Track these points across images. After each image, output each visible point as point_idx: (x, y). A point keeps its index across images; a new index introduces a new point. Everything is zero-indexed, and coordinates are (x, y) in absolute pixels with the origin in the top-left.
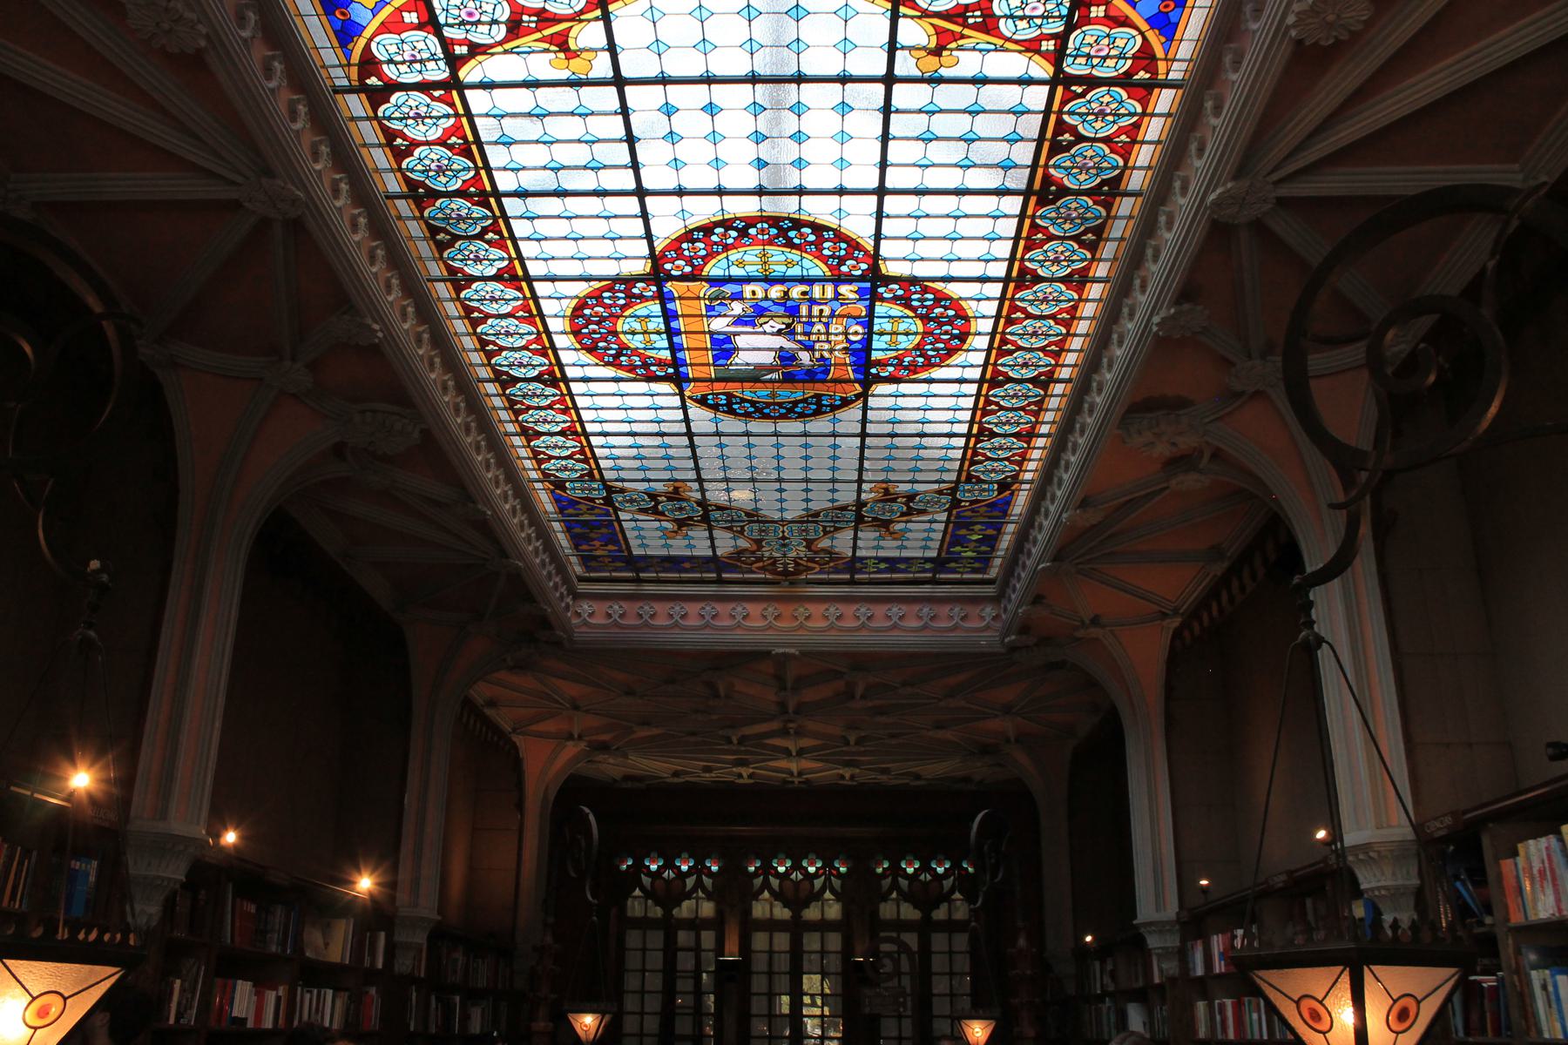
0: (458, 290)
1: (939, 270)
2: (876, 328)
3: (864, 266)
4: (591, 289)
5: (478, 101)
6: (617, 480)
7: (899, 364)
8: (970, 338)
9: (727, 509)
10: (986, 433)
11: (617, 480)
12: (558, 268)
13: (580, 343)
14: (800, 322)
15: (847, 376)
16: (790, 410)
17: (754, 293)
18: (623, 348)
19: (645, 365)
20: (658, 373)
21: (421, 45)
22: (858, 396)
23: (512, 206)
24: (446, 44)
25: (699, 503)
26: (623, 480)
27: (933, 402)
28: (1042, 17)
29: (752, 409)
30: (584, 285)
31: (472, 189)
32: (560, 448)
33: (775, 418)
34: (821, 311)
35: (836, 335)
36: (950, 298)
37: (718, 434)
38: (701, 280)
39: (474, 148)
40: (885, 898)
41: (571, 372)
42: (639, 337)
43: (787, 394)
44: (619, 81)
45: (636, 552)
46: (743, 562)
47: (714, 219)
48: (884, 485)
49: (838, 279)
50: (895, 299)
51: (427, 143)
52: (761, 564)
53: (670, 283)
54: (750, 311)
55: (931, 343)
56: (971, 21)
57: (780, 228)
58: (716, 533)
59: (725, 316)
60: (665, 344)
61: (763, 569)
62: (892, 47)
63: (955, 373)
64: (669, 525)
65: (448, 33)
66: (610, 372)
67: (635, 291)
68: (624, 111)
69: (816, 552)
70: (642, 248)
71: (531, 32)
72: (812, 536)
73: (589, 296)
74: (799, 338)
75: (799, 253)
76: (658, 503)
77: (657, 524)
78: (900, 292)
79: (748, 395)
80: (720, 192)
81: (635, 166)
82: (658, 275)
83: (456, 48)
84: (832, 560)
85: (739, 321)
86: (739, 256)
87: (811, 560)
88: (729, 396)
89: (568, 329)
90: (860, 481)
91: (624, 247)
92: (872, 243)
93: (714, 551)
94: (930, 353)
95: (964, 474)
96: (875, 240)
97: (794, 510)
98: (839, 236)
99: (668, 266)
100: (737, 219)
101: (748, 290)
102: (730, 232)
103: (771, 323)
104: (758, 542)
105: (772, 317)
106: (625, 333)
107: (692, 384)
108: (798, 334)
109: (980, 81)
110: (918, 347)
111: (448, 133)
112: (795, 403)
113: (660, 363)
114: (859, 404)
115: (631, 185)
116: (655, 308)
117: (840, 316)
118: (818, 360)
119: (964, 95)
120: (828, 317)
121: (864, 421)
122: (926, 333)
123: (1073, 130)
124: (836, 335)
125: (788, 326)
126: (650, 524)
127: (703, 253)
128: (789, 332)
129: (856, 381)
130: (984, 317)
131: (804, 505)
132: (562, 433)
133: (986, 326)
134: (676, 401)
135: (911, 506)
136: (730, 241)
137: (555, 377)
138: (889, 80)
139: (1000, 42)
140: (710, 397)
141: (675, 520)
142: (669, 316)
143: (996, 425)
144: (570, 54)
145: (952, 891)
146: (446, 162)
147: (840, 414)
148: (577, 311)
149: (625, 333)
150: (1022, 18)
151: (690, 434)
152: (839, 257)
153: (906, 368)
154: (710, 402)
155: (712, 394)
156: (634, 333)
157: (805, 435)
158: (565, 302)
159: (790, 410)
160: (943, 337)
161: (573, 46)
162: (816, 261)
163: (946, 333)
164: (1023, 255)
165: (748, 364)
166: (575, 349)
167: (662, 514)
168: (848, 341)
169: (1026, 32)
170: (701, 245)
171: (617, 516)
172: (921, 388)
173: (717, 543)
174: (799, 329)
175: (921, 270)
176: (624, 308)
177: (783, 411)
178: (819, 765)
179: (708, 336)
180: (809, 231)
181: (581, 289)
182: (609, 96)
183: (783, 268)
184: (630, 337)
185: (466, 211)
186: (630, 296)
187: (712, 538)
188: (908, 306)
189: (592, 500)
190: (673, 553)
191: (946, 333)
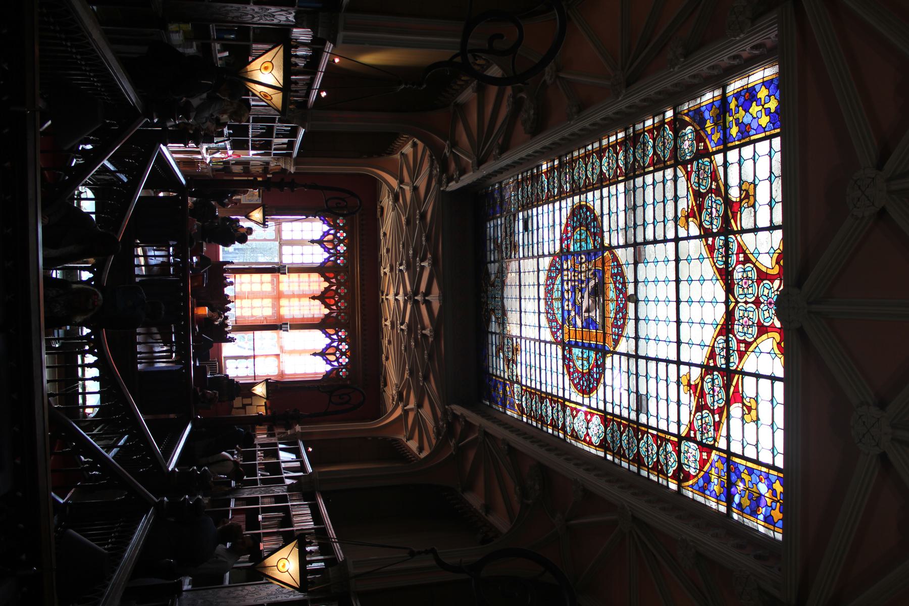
0: (596, 152)
1: (608, 381)
2: (584, 351)
5: (669, 173)
7: (570, 360)
10: (542, 400)
18: (574, 229)
19: (567, 238)
20: (564, 244)
27: (554, 375)
28: (702, 431)
29: (549, 288)
36: (597, 386)
37: (539, 271)
41: (564, 203)
42: (578, 237)
44: (677, 240)
48: (519, 349)
50: (596, 360)
52: (484, 285)
57: (623, 308)
62: (690, 365)
63: (567, 387)
65: (695, 163)
66: (564, 221)
68: (665, 241)
71: (696, 201)
78: (599, 363)
80: (636, 282)
100: (626, 288)
106: (580, 230)
109: (679, 403)
113: (568, 246)
114: (553, 340)
119: (673, 397)
121: (546, 342)
122: (583, 374)
130: (590, 401)
136: (618, 285)
138: (678, 363)
139: (693, 413)
143: (546, 405)
144: (687, 217)
148: (588, 208)
151: (539, 256)
153: (569, 363)
156: (580, 235)
158: (592, 203)
160: (581, 382)
161: (690, 219)
163: (583, 383)
164: (615, 421)
166: (573, 206)
169: (697, 424)
172: (560, 370)
173: (492, 264)
175: (608, 373)
177: (549, 303)
181: (597, 211)
182: (671, 235)
184: (579, 233)
186: (595, 234)
191: (583, 383)
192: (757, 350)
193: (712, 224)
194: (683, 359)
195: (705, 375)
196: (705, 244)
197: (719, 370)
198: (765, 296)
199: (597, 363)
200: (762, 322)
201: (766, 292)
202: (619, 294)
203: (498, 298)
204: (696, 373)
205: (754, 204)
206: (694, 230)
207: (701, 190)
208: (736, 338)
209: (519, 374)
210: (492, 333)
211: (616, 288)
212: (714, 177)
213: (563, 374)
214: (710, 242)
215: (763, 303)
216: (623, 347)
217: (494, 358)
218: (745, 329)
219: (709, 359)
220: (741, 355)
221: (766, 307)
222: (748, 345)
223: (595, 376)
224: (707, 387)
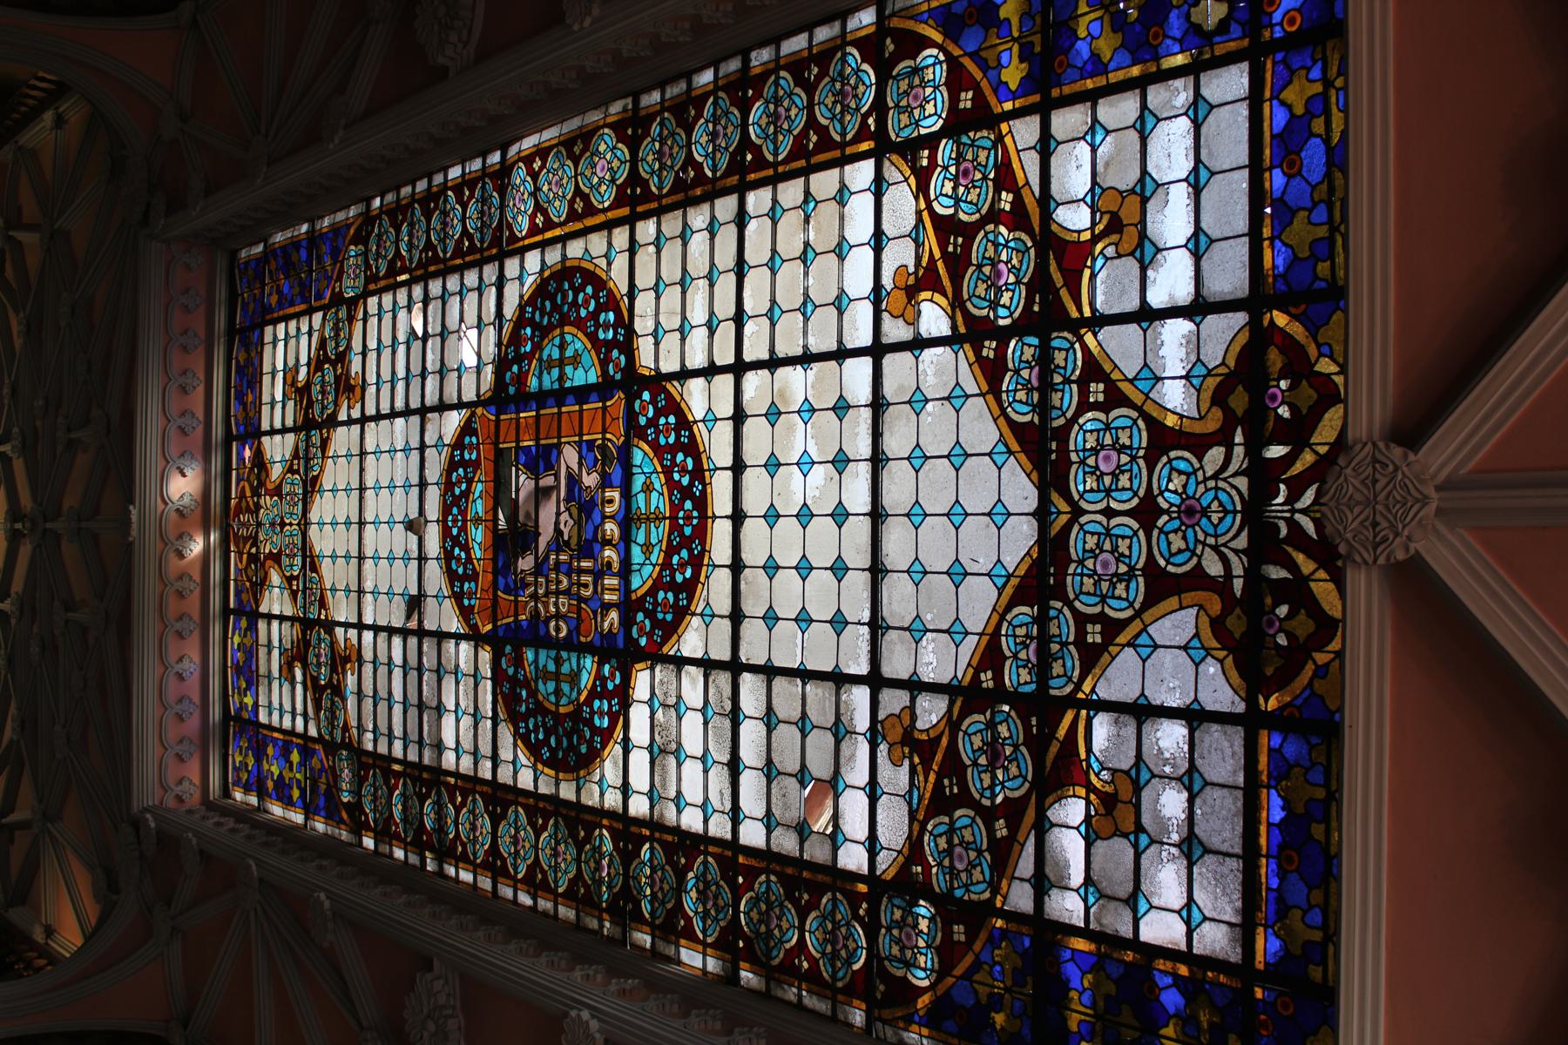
2: (564, 654)
3: (643, 642)
4: (619, 297)
6: (366, 312)
8: (552, 773)
9: (323, 452)
11: (366, 312)
12: (645, 257)
13: (552, 276)
14: (571, 557)
15: (500, 617)
17: (611, 501)
19: (519, 358)
20: (509, 374)
21: (930, 109)
22: (474, 628)
23: (726, 207)
24: (932, 141)
25: (334, 415)
26: (365, 321)
29: (457, 491)
30: (624, 289)
31: (749, 157)
32: (410, 241)
33: (445, 521)
34: (586, 586)
35: (556, 604)
38: (627, 435)
39: (802, 163)
41: (512, 266)
42: (556, 354)
44: (878, 350)
45: (269, 330)
46: (251, 469)
47: (704, 457)
48: (354, 658)
49: (629, 606)
50: (599, 676)
51: (810, 107)
52: (248, 494)
53: (622, 396)
54: (586, 496)
55: (544, 723)
56: (946, 782)
57: (691, 539)
58: (290, 437)
59: (580, 464)
60: (547, 384)
61: (242, 496)
62: (915, 686)
63: (506, 754)
64: (303, 374)
66: (509, 310)
67: (615, 353)
69: (263, 565)
70: (669, 365)
71: (943, 245)
72: (285, 561)
73: (610, 292)
74: (553, 557)
75: (660, 561)
76: (334, 364)
77: (304, 360)
78: (610, 686)
79: (478, 488)
80: (738, 467)
81: (773, 363)
82: (633, 381)
83: (926, 153)
84: (253, 584)
85: (573, 481)
86: (657, 486)
87: (253, 558)
89: (568, 264)
91: (671, 342)
92: (672, 653)
93: (267, 433)
94: (531, 722)
96: (675, 656)
97: (322, 542)
98: (682, 613)
99: (646, 396)
100: (705, 485)
101: (616, 495)
102: (687, 477)
103: (571, 522)
104: (277, 491)
105: (578, 523)
107: (493, 418)
108: (557, 555)
110: (540, 709)
111: (823, 132)
112: (466, 548)
113: (521, 379)
115: (748, 357)
116: (593, 378)
117: (579, 609)
118: (523, 579)
119: (858, 773)
120: (578, 593)
122: (557, 717)
123: (814, 904)
124: (556, 604)
125: (567, 543)
127: (662, 441)
128: (558, 543)
129: (495, 627)
132: (429, 245)
133: (567, 792)
134: (469, 395)
135: (326, 694)
136: (676, 476)
137: (503, 246)
140: (474, 440)
141: (308, 384)
142: (582, 393)
146: (786, 126)
147: (448, 604)
149: (562, 335)
150: (950, 842)
152: (654, 611)
153: (512, 689)
154: (467, 440)
155: (478, 444)
158: (603, 263)
159: (456, 541)
160: (553, 741)
162: (650, 582)
165: (517, 490)
166: (542, 271)
167: (319, 368)
168: (548, 620)
170: (671, 440)
171: (317, 310)
173: (278, 438)
174: (563, 557)
176: (592, 337)
177: (455, 531)
179: (555, 441)
180: (688, 574)
183: (641, 539)
184: (557, 341)
185: (723, 145)
186: (611, 345)
187: (284, 430)
188: (593, 694)
189: (340, 279)
190: (266, 379)
191: (559, 742)
192: (1143, 639)
193: (994, 305)
194: (888, 671)
195: (964, 714)
196: (972, 359)
197: (1015, 698)
198: (1175, 492)
199: (604, 686)
200: (1162, 563)
201: (1177, 483)
202: (682, 501)
203: (291, 524)
204: (931, 711)
205: (1140, 245)
206: (934, 318)
207: (962, 216)
208: (1074, 611)
209: (354, 723)
210: (270, 617)
211: (671, 484)
212: (1005, 177)
213: (495, 718)
214: (988, 351)
215: (1167, 512)
216: (691, 642)
218: (1105, 585)
219: (978, 670)
220: (1092, 658)
221: (1176, 523)
222: (1112, 628)
223: (597, 722)
224: (969, 746)
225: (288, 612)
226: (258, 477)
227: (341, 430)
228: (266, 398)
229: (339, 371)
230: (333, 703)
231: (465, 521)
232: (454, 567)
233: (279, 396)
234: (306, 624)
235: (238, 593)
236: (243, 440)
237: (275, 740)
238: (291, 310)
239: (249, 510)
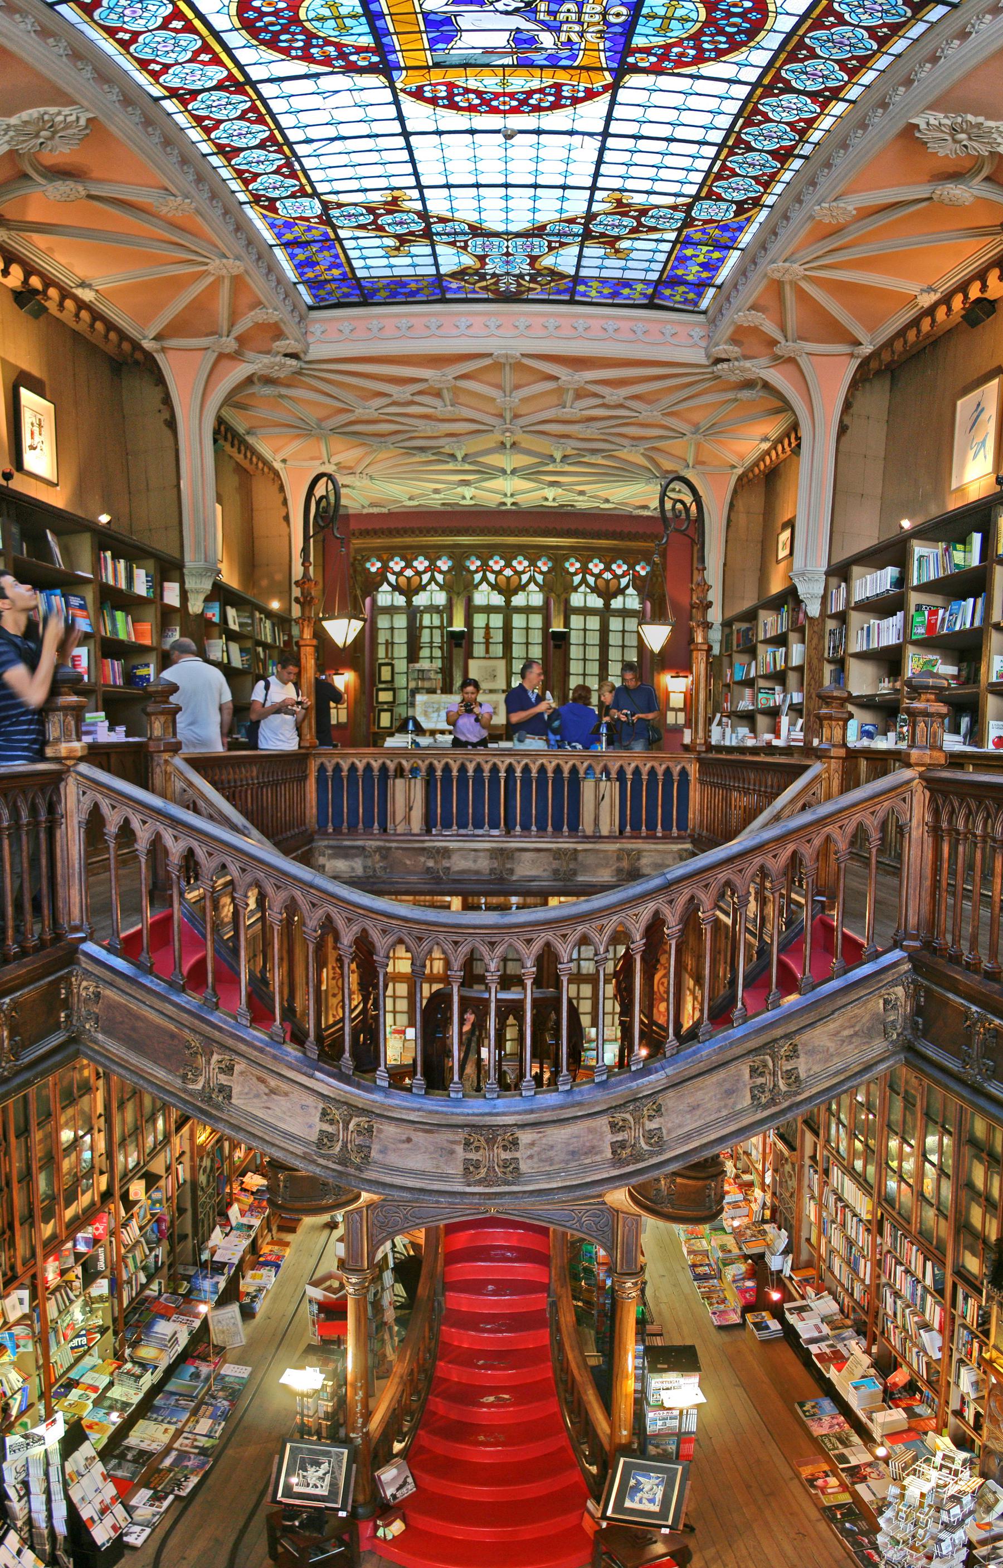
16: (523, 102)
25: (418, 213)
29: (477, 101)
33: (505, 112)
40: (575, 589)
43: (519, 82)
46: (466, 281)
48: (617, 195)
52: (484, 284)
58: (440, 249)
64: (390, 242)
69: (539, 273)
72: (536, 252)
76: (377, 216)
77: (377, 242)
79: (472, 84)
87: (533, 280)
88: (450, 86)
90: (593, 188)
93: (438, 269)
95: (705, 189)
104: (482, 259)
126: (371, 242)
131: (530, 216)
145: (627, 587)
154: (428, 95)
157: (539, 132)
159: (523, 102)
167: (380, 228)
173: (440, 260)
177: (514, 103)
178: (531, 485)
187: (434, 254)
190: (397, 272)
217: (630, 264)
225: (575, 250)
226: (471, 275)
227: (429, 207)
228: (410, 271)
229: (382, 211)
230: (652, 217)
231: (504, 94)
232: (548, 104)
233: (408, 261)
234: (587, 235)
235: (559, 292)
236: (444, 290)
237: (673, 268)
238: (342, 256)
239: (496, 283)
